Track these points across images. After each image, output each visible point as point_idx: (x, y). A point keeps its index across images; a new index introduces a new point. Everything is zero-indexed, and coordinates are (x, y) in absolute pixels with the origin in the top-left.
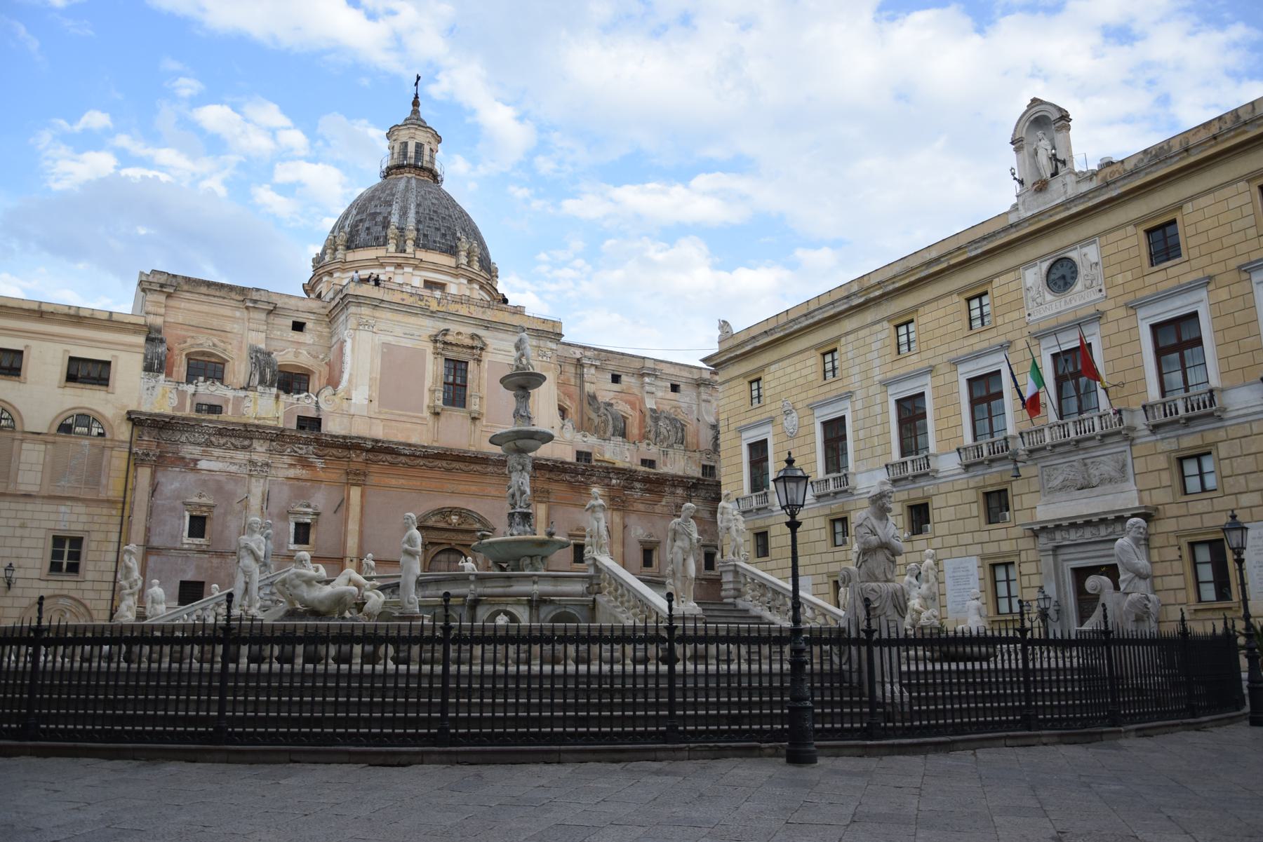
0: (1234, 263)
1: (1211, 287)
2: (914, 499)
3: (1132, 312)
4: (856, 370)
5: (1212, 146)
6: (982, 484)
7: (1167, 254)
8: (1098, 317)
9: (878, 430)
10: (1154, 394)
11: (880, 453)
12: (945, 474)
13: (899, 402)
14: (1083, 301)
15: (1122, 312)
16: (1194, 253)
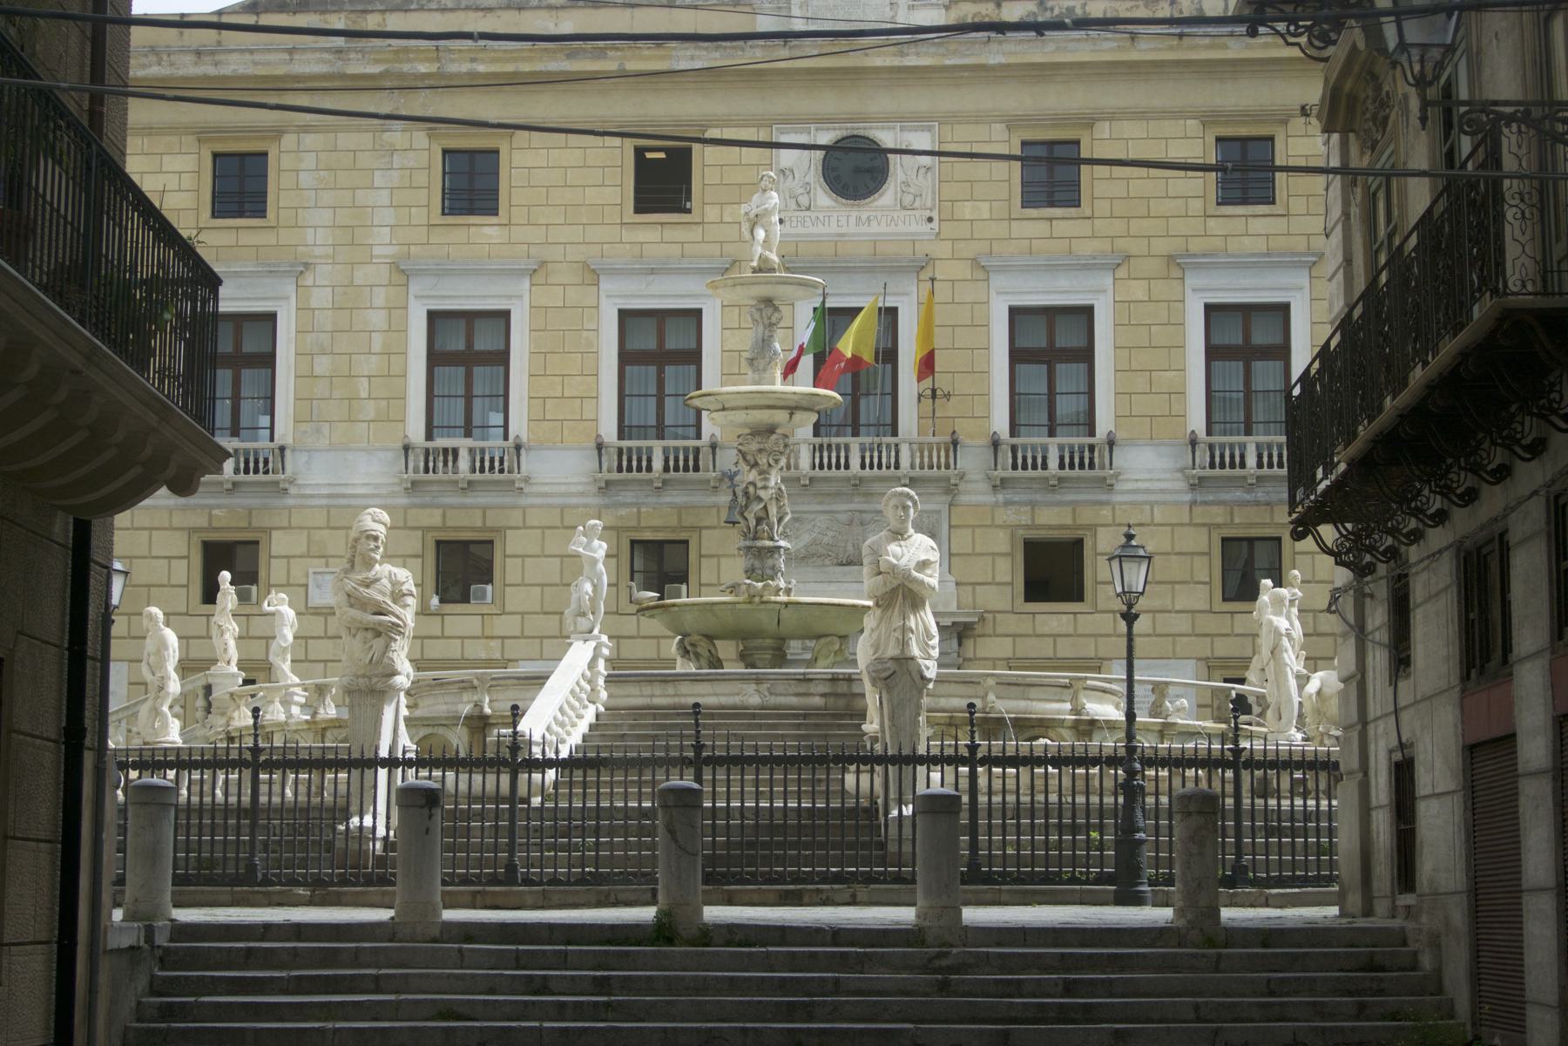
0: (1162, 246)
1: (1121, 273)
2: (456, 529)
3: (981, 275)
4: (326, 216)
5: (1171, 48)
6: (634, 523)
7: (1051, 194)
8: (920, 267)
9: (371, 365)
10: (1000, 422)
11: (372, 415)
12: (546, 489)
13: (433, 316)
14: (892, 229)
15: (962, 270)
16: (1102, 207)
